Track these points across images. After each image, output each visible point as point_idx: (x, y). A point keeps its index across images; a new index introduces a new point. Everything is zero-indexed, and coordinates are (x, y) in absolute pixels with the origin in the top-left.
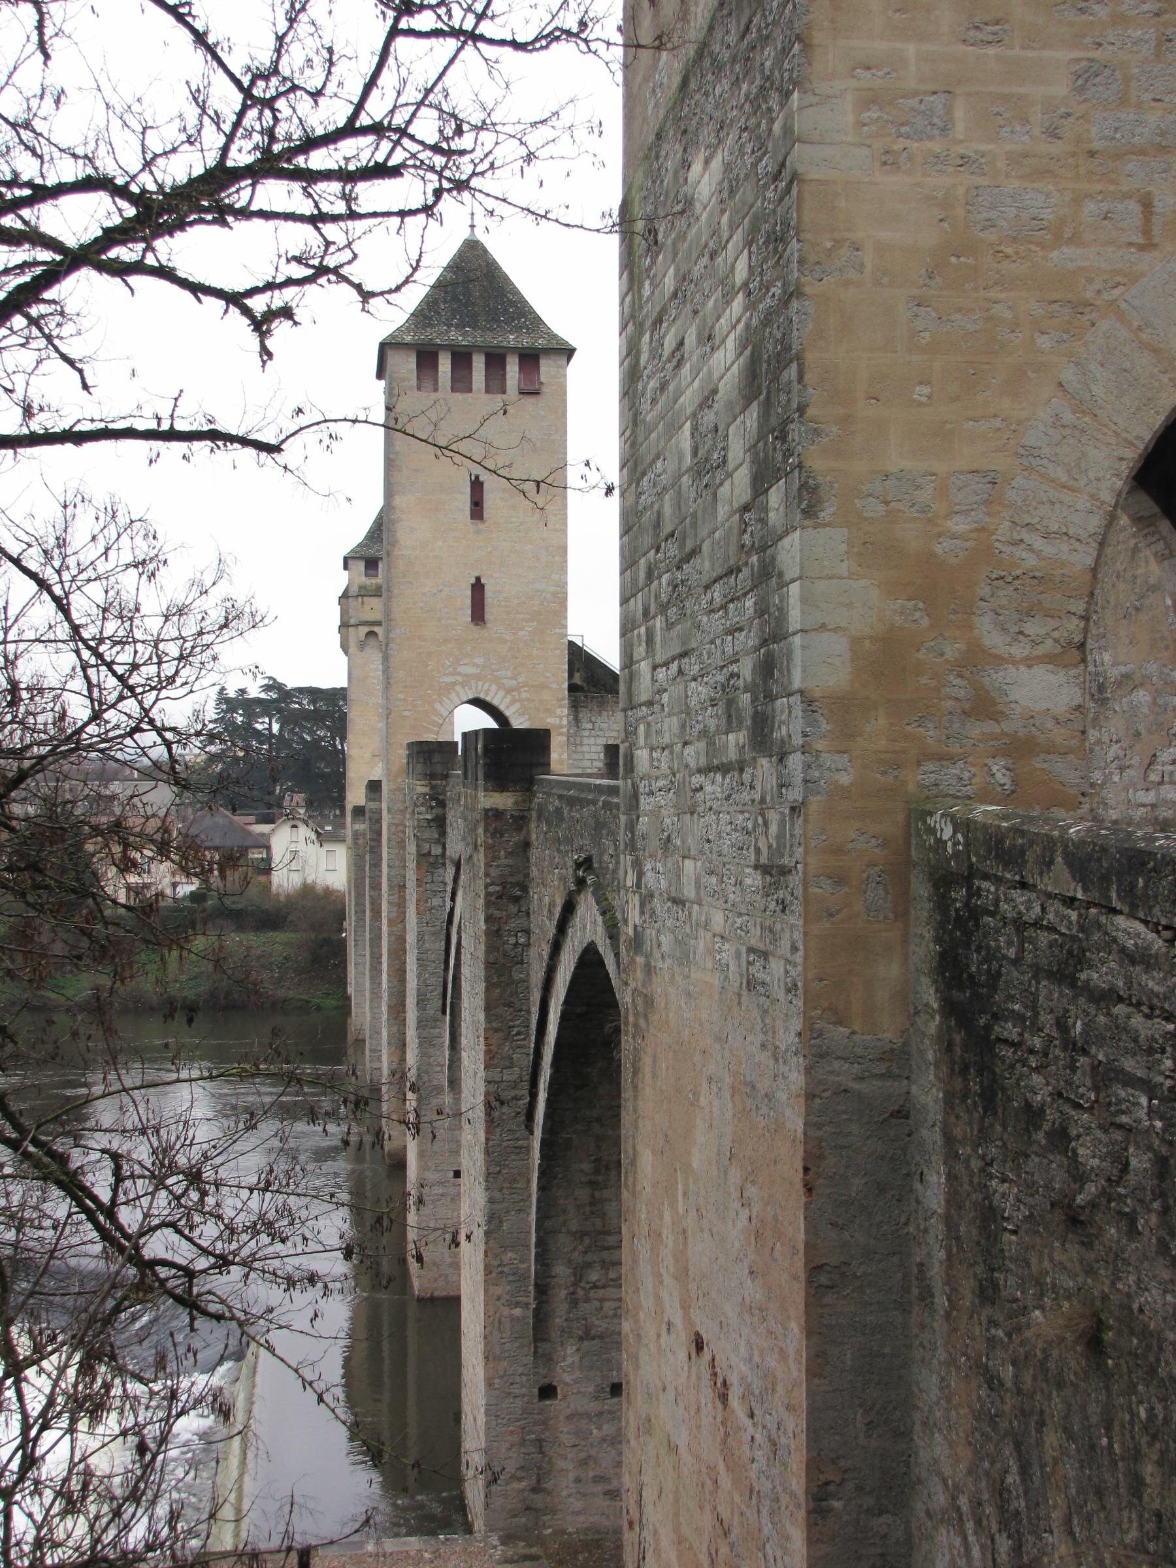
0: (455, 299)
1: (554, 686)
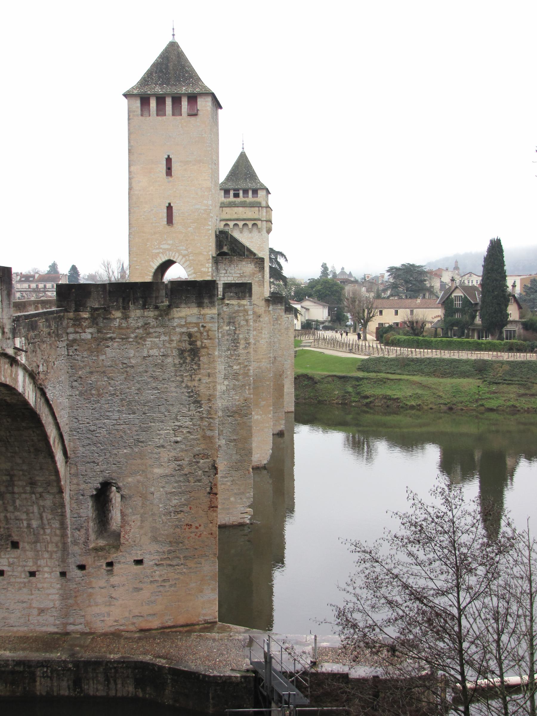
0: (161, 71)
1: (205, 253)
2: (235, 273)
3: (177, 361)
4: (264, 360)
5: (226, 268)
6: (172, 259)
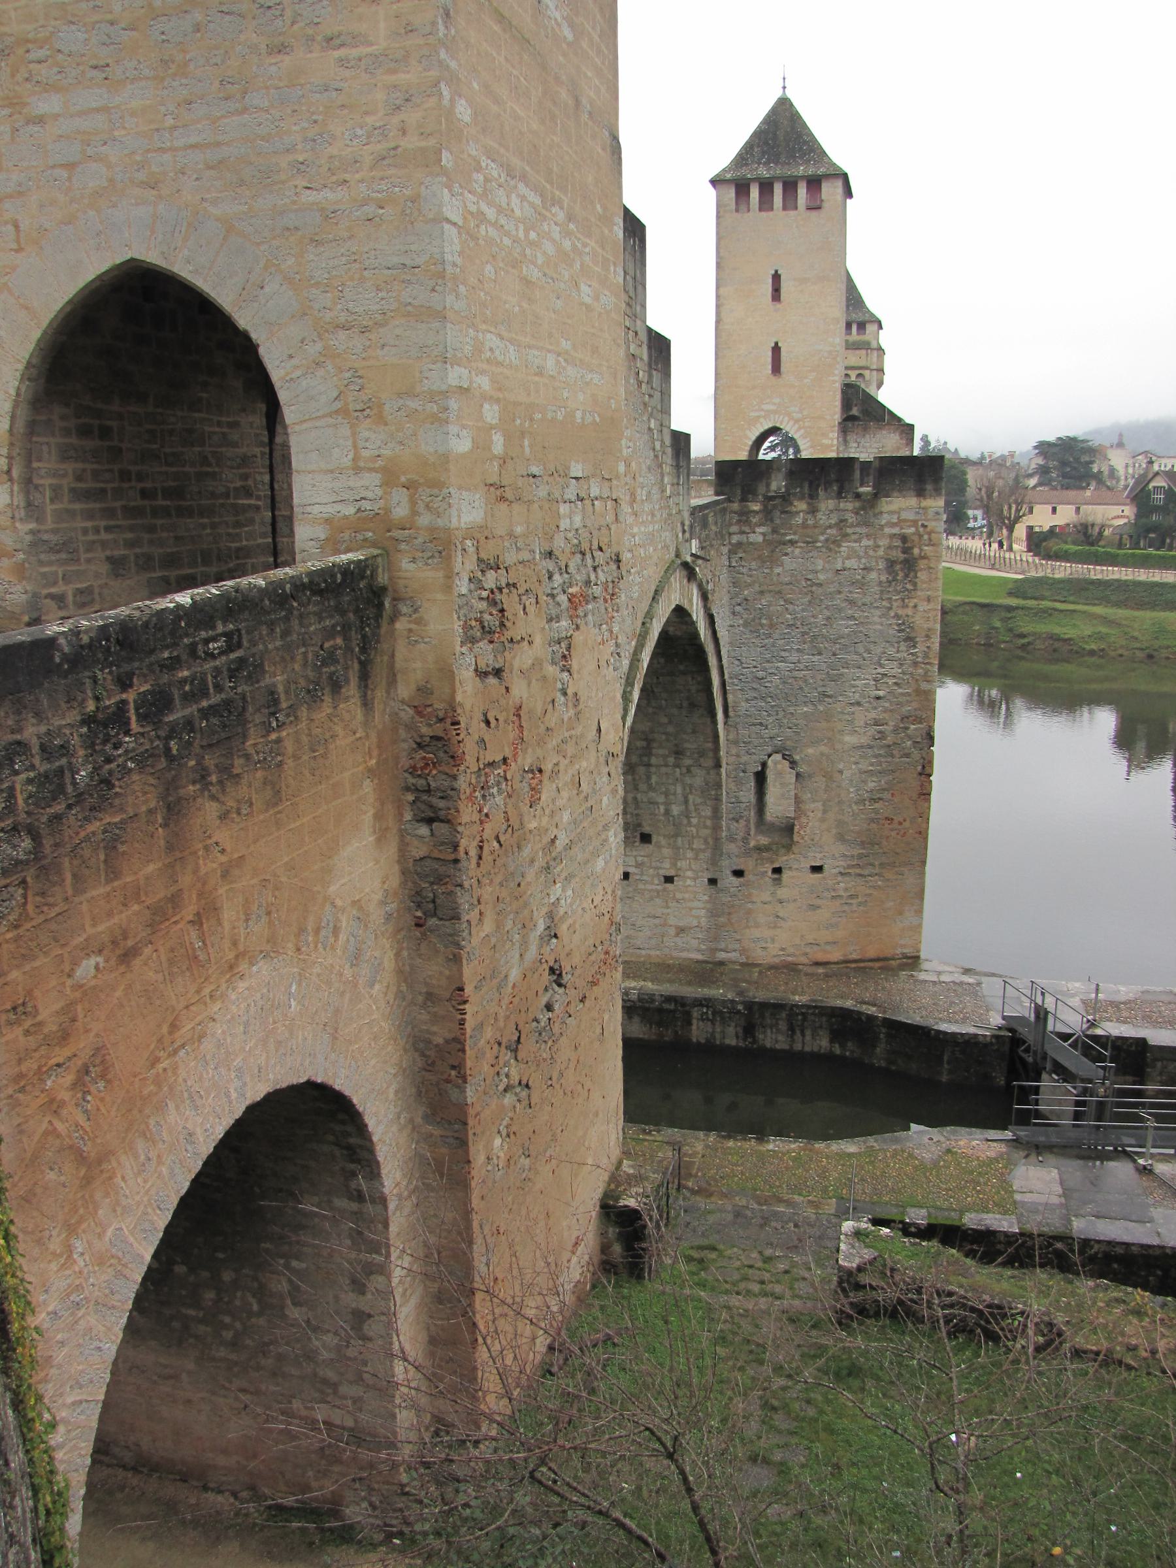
0: (766, 143)
6: (778, 425)
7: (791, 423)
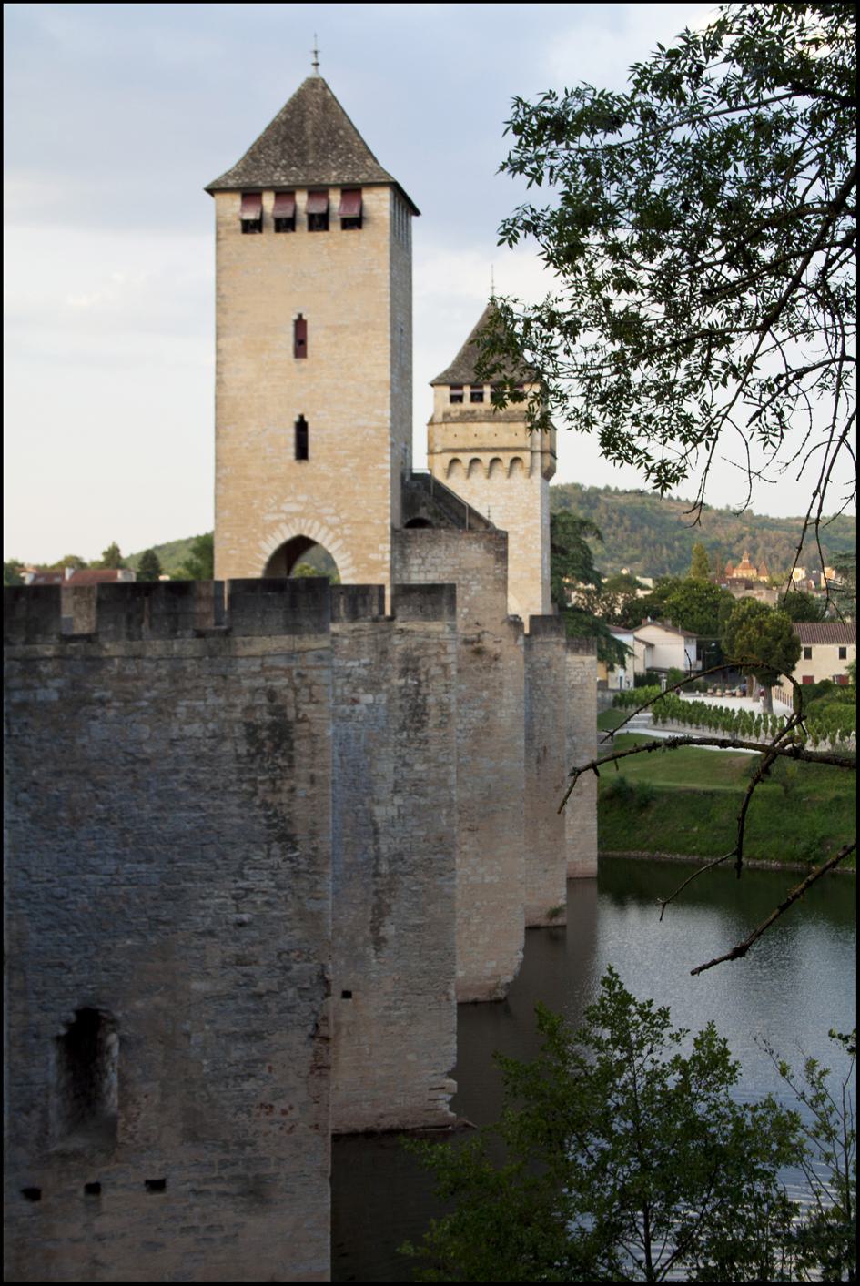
1: (377, 522)
2: (441, 564)
3: (243, 750)
4: (505, 754)
5: (423, 554)
6: (305, 534)
7: (324, 530)
